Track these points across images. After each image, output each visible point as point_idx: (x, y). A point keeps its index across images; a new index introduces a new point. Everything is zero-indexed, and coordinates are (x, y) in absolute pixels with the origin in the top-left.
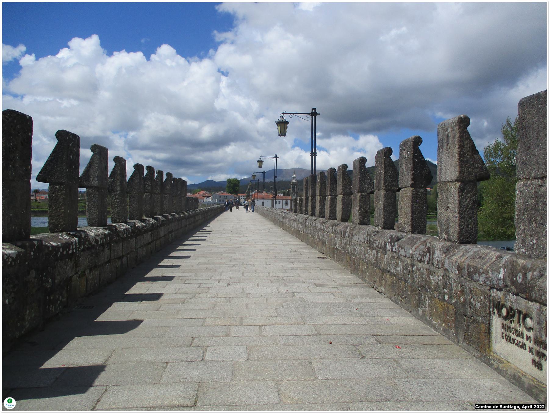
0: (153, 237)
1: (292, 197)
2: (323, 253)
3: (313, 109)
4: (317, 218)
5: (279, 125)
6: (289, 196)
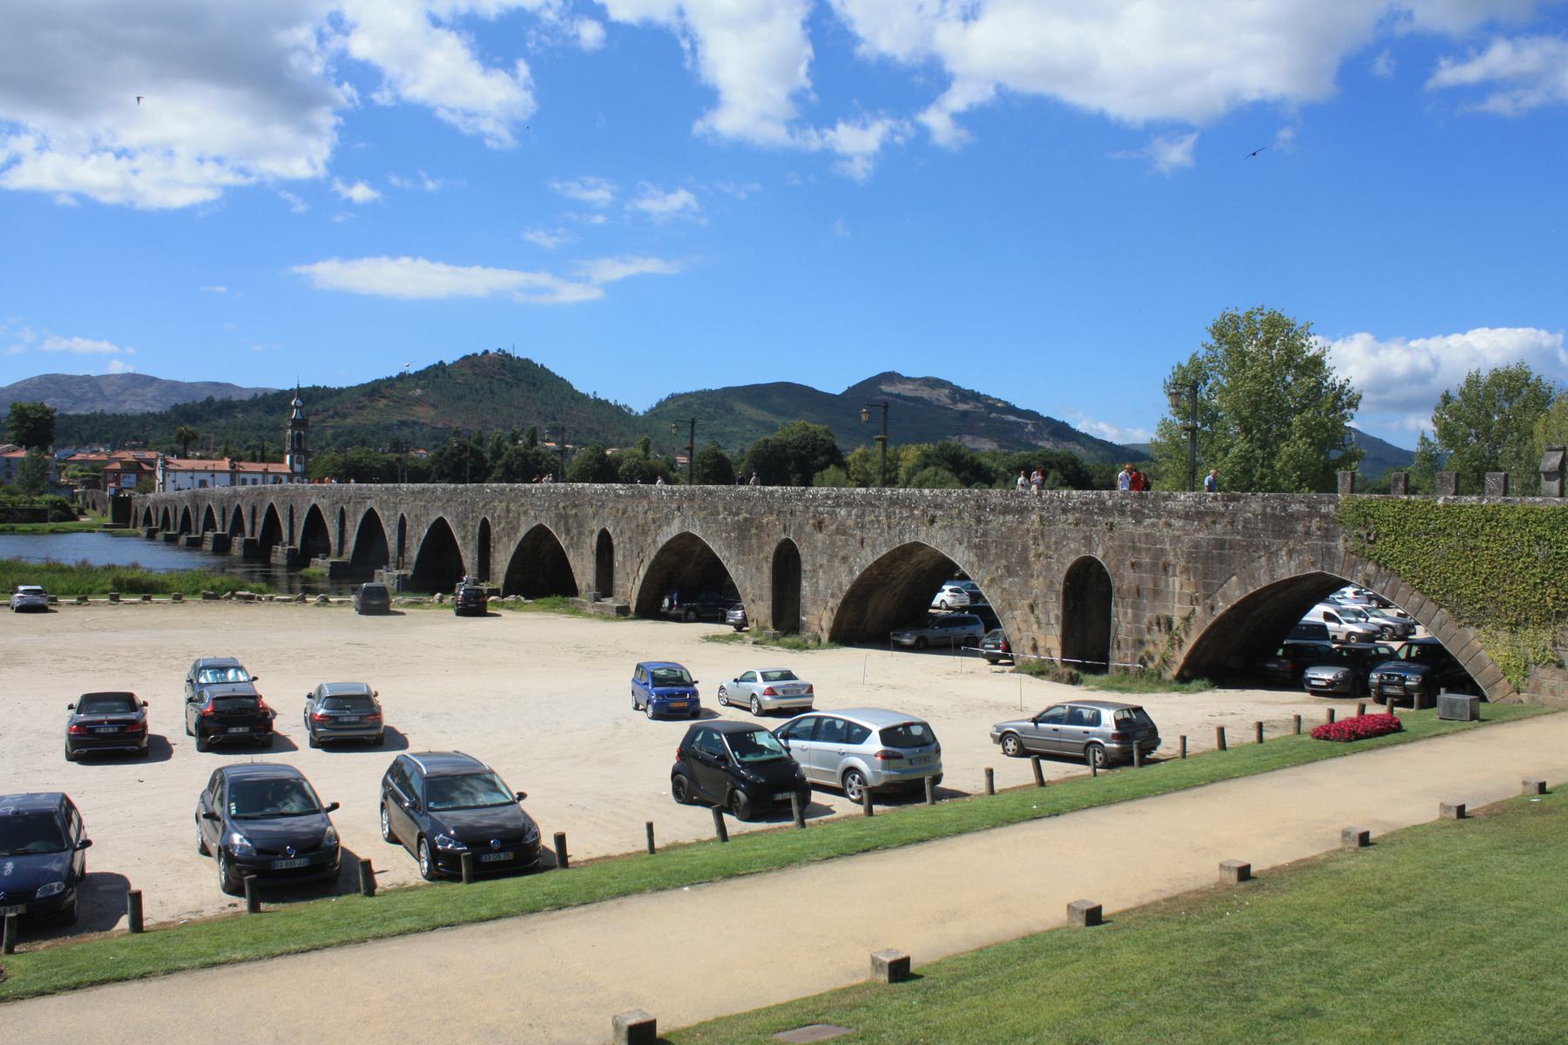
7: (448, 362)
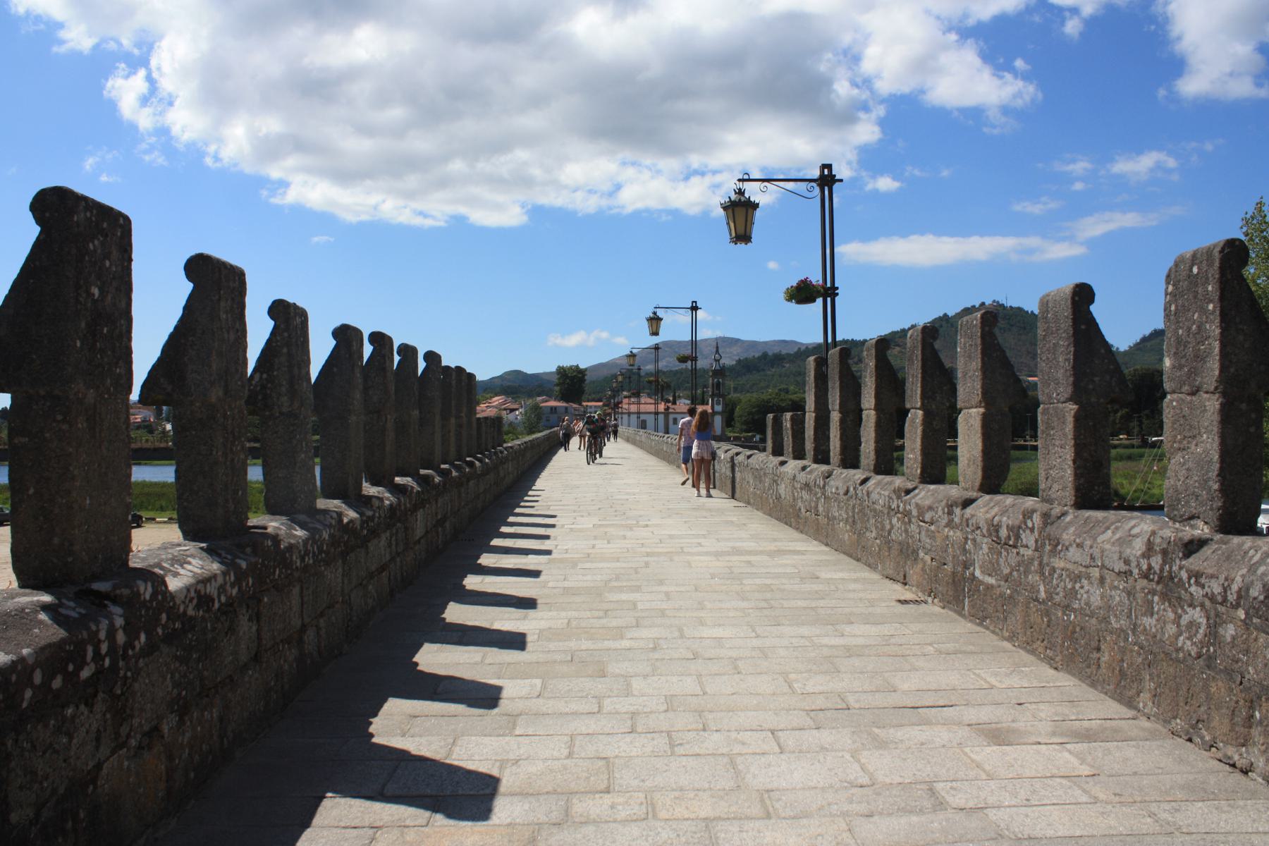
0: (394, 547)
1: (713, 408)
2: (905, 584)
3: (824, 166)
4: (872, 474)
5: (730, 211)
6: (707, 404)
7: (951, 314)
